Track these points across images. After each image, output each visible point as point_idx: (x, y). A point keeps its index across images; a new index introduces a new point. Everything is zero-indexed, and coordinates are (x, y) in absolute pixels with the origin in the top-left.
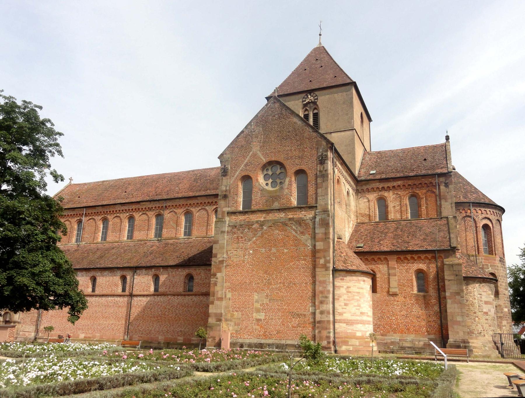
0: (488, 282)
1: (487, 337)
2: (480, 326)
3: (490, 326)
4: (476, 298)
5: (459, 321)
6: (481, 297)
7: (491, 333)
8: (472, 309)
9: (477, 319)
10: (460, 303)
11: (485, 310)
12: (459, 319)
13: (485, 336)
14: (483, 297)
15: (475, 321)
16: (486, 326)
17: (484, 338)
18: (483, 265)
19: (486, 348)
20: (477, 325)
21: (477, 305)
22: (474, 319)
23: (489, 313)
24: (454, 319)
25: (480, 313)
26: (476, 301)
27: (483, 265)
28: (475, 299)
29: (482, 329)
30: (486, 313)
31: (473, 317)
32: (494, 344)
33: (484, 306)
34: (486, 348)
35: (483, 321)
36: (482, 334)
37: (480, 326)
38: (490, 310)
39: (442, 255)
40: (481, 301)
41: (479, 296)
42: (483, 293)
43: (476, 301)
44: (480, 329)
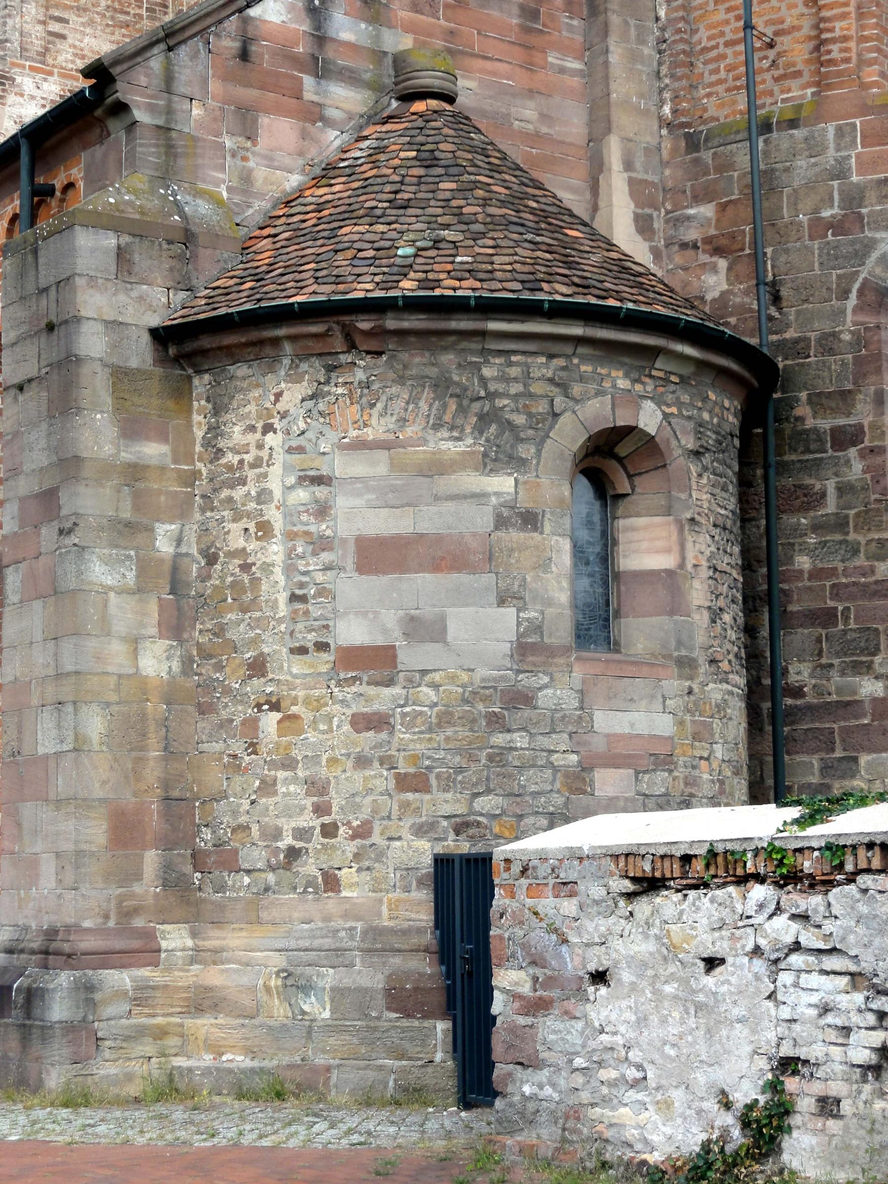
0: (378, 344)
1: (354, 887)
2: (290, 787)
3: (413, 782)
4: (278, 523)
5: (46, 757)
6: (322, 511)
7: (423, 852)
8: (238, 633)
9: (270, 721)
10: (56, 593)
11: (352, 632)
12: (46, 739)
13: (331, 882)
14: (342, 503)
15: (253, 748)
16: (360, 790)
17: (331, 903)
18: (853, 199)
19: (310, 1004)
20: (268, 787)
21: (276, 590)
22: (251, 724)
23: (410, 657)
24: (26, 750)
25: (297, 666)
26: (276, 551)
27: (853, 199)
28: (265, 530)
29: (308, 820)
30: (374, 662)
31: (240, 713)
32: (426, 967)
33: (351, 587)
34: (310, 1004)
35: (329, 734)
36: (309, 867)
37: (290, 787)
38: (425, 629)
39: (77, 173)
40: (321, 544)
41: (302, 495)
42: (341, 466)
43: (276, 551)
44: (289, 810)
